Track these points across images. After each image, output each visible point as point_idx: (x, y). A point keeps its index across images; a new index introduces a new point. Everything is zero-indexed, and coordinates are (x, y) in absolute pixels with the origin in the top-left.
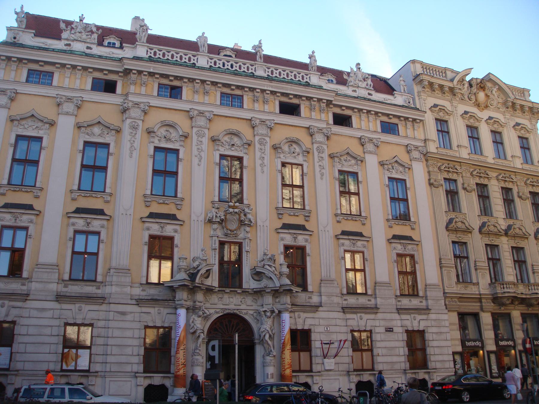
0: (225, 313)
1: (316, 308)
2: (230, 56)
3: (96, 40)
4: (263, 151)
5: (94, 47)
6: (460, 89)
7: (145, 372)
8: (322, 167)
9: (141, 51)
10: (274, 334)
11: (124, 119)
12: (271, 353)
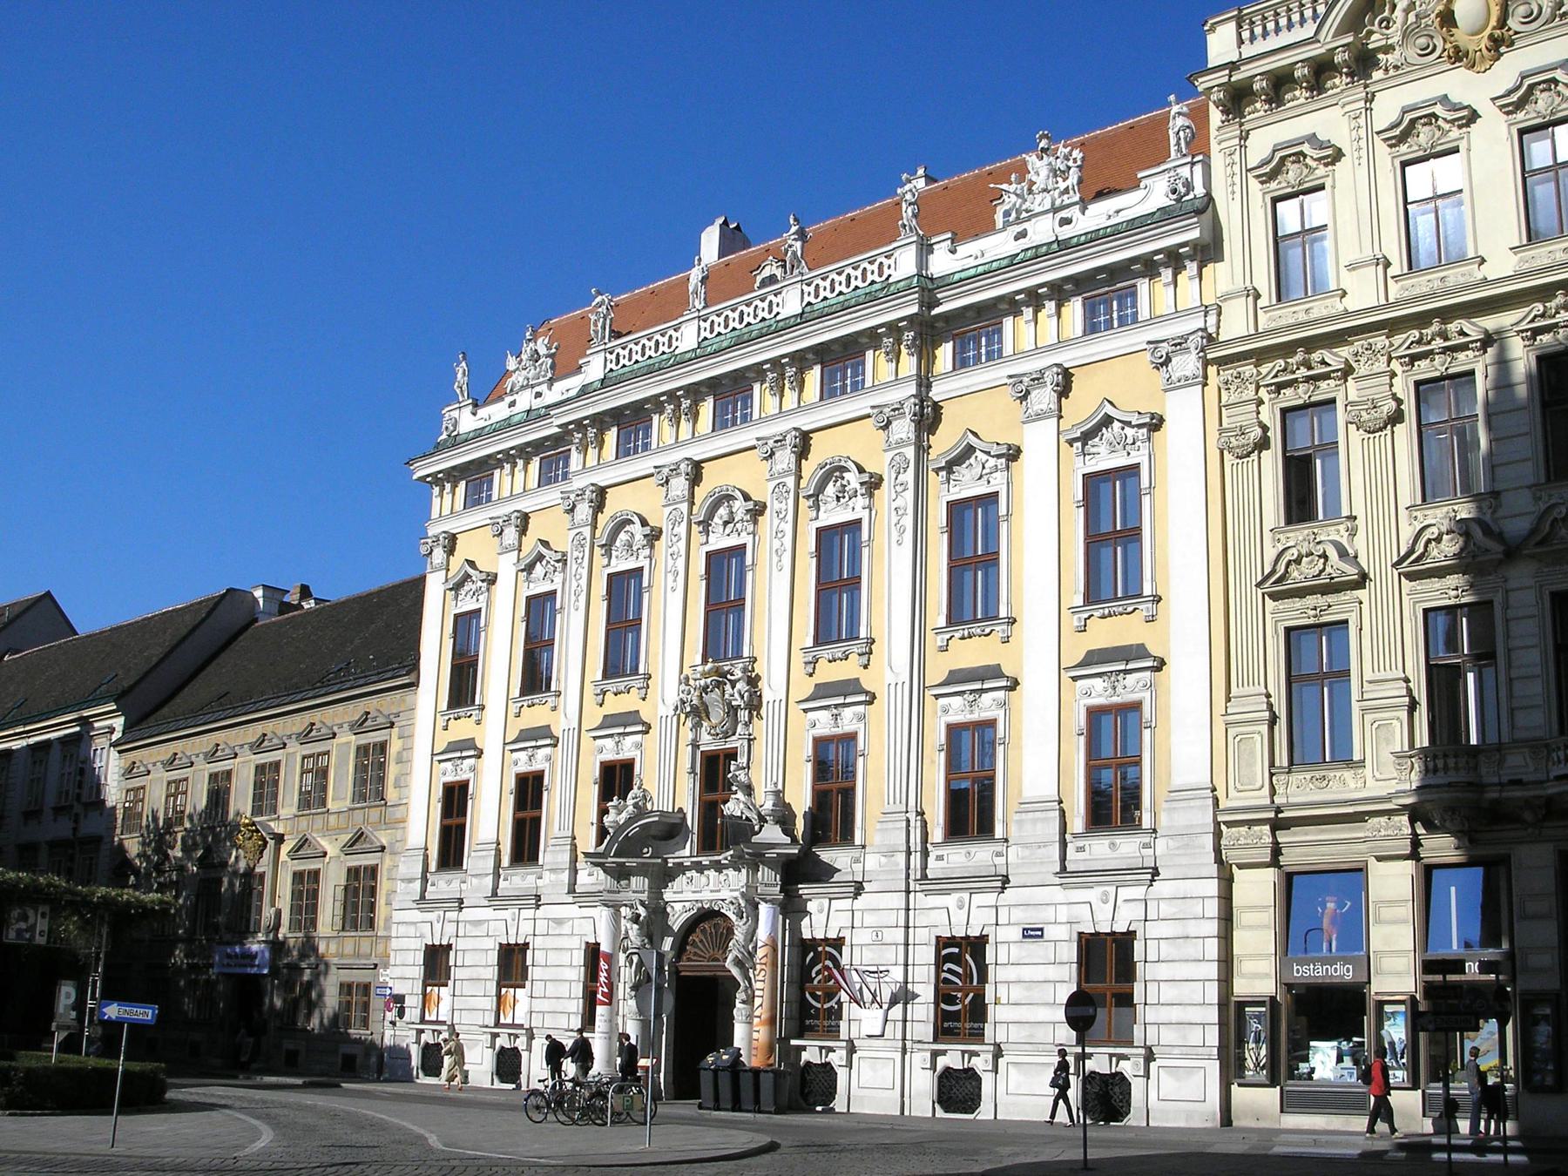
2: (772, 279)
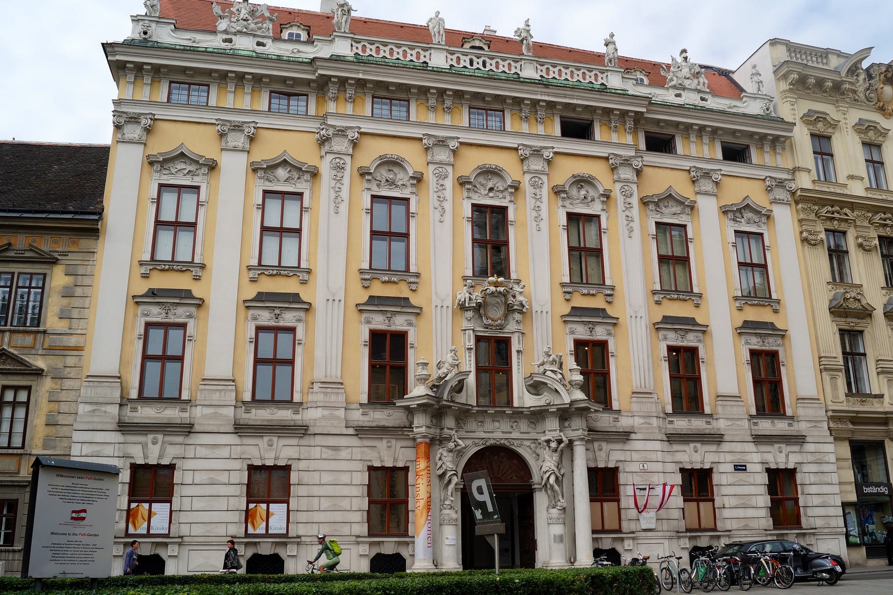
0: (488, 444)
1: (625, 436)
2: (481, 48)
3: (271, 31)
4: (538, 197)
5: (268, 42)
6: (850, 83)
7: (370, 535)
8: (629, 219)
9: (343, 48)
10: (563, 476)
11: (323, 154)
12: (559, 504)
